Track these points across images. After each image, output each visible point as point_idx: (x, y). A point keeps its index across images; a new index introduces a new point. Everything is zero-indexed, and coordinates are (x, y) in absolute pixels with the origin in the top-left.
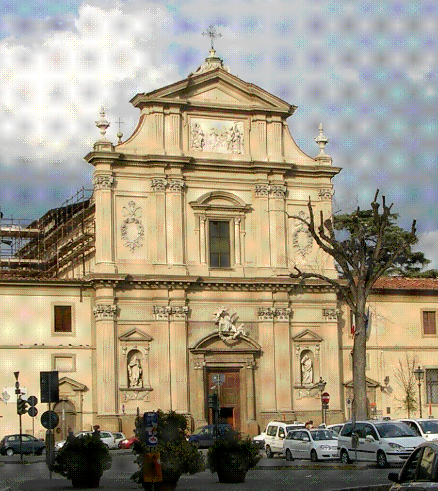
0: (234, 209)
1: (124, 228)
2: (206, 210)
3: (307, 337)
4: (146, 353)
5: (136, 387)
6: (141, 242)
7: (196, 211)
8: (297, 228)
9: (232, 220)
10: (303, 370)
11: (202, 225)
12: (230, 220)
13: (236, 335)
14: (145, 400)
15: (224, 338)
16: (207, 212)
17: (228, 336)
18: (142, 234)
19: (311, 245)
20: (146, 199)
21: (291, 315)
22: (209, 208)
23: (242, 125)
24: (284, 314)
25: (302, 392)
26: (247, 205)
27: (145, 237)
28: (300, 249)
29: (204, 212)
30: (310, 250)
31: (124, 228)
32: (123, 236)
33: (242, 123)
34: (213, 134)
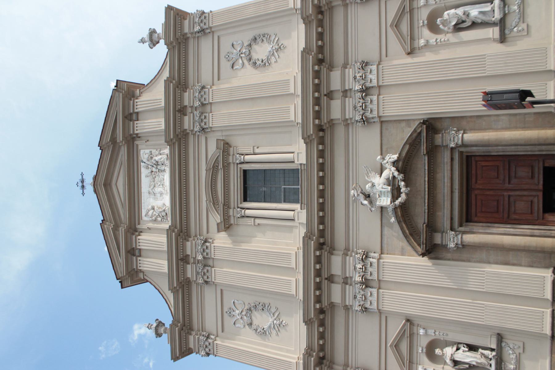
0: (226, 166)
1: (256, 330)
2: (229, 207)
3: (405, 27)
4: (433, 334)
5: (493, 362)
6: (273, 310)
7: (232, 222)
8: (246, 62)
9: (239, 166)
10: (468, 24)
11: (248, 212)
12: (240, 168)
13: (396, 174)
14: (521, 351)
15: (403, 197)
16: (232, 206)
17: (399, 188)
18: (264, 305)
19: (266, 36)
20: (224, 292)
21: (365, 64)
22: (227, 205)
23: (144, 154)
24: (364, 78)
25: (511, 21)
26: (217, 148)
27: (267, 301)
28: (273, 54)
29: (231, 211)
30: (272, 38)
31: (256, 330)
32: (267, 333)
33: (141, 151)
34: (153, 190)
